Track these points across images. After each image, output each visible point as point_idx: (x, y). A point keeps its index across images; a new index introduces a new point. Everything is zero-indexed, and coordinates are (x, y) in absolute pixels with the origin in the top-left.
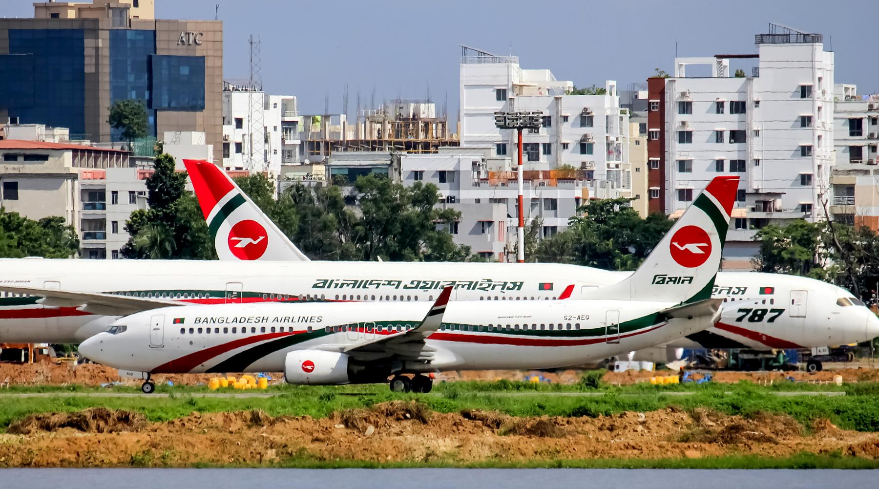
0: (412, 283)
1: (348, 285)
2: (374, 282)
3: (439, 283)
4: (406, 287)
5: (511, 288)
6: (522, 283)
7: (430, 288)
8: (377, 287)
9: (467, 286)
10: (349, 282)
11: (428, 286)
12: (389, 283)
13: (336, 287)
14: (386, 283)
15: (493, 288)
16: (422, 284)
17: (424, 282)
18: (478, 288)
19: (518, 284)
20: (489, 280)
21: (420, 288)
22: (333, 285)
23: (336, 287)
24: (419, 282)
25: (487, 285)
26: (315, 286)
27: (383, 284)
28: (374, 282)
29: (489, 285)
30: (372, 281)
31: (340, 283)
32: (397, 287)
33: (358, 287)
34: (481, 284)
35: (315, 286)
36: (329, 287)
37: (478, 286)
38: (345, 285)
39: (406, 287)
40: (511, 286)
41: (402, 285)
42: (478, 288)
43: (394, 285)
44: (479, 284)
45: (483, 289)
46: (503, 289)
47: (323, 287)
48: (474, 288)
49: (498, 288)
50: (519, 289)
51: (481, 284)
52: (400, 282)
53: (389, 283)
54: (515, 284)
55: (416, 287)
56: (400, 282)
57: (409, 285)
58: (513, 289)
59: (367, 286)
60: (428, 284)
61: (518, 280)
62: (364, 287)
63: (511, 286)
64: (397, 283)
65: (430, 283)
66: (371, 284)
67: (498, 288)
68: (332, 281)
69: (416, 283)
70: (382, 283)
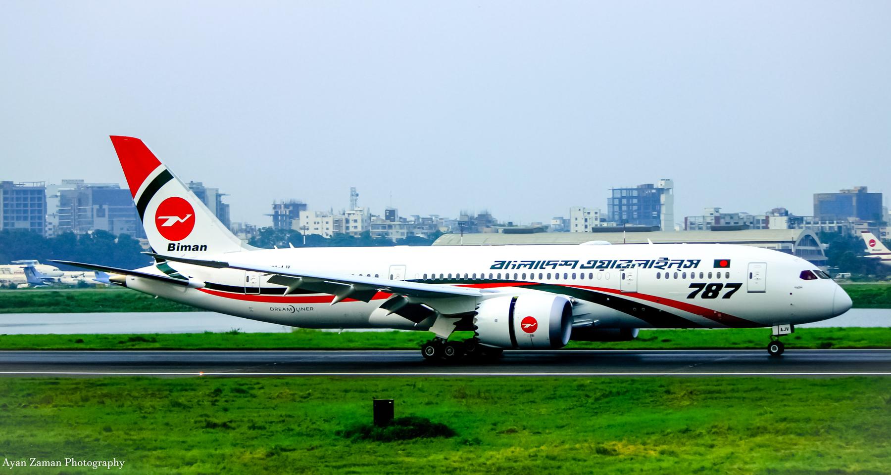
0: (589, 263)
1: (525, 266)
2: (551, 263)
3: (616, 261)
4: (582, 267)
5: (687, 265)
6: (699, 261)
7: (607, 267)
8: (554, 268)
9: (643, 265)
10: (526, 263)
11: (605, 265)
12: (566, 263)
13: (513, 268)
14: (563, 263)
15: (670, 267)
16: (598, 264)
17: (601, 262)
18: (655, 267)
19: (695, 262)
20: (666, 259)
21: (597, 268)
22: (511, 266)
23: (513, 268)
24: (596, 262)
25: (663, 264)
26: (493, 267)
27: (561, 265)
28: (551, 263)
29: (666, 263)
30: (549, 262)
31: (517, 264)
32: (574, 267)
33: (536, 268)
34: (658, 263)
35: (493, 267)
36: (506, 268)
37: (654, 264)
38: (523, 266)
39: (582, 267)
40: (688, 264)
41: (579, 265)
42: (655, 267)
43: (570, 265)
44: (655, 262)
45: (660, 267)
46: (679, 267)
47: (501, 268)
48: (650, 267)
49: (675, 266)
50: (696, 267)
51: (658, 263)
52: (576, 262)
53: (566, 263)
54: (691, 261)
55: (592, 267)
56: (576, 262)
57: (586, 265)
58: (689, 267)
59: (544, 266)
60: (604, 263)
61: (695, 258)
62: (541, 268)
63: (688, 264)
64: (573, 263)
65: (606, 263)
66: (548, 264)
67: (675, 266)
68: (510, 262)
70: (560, 263)
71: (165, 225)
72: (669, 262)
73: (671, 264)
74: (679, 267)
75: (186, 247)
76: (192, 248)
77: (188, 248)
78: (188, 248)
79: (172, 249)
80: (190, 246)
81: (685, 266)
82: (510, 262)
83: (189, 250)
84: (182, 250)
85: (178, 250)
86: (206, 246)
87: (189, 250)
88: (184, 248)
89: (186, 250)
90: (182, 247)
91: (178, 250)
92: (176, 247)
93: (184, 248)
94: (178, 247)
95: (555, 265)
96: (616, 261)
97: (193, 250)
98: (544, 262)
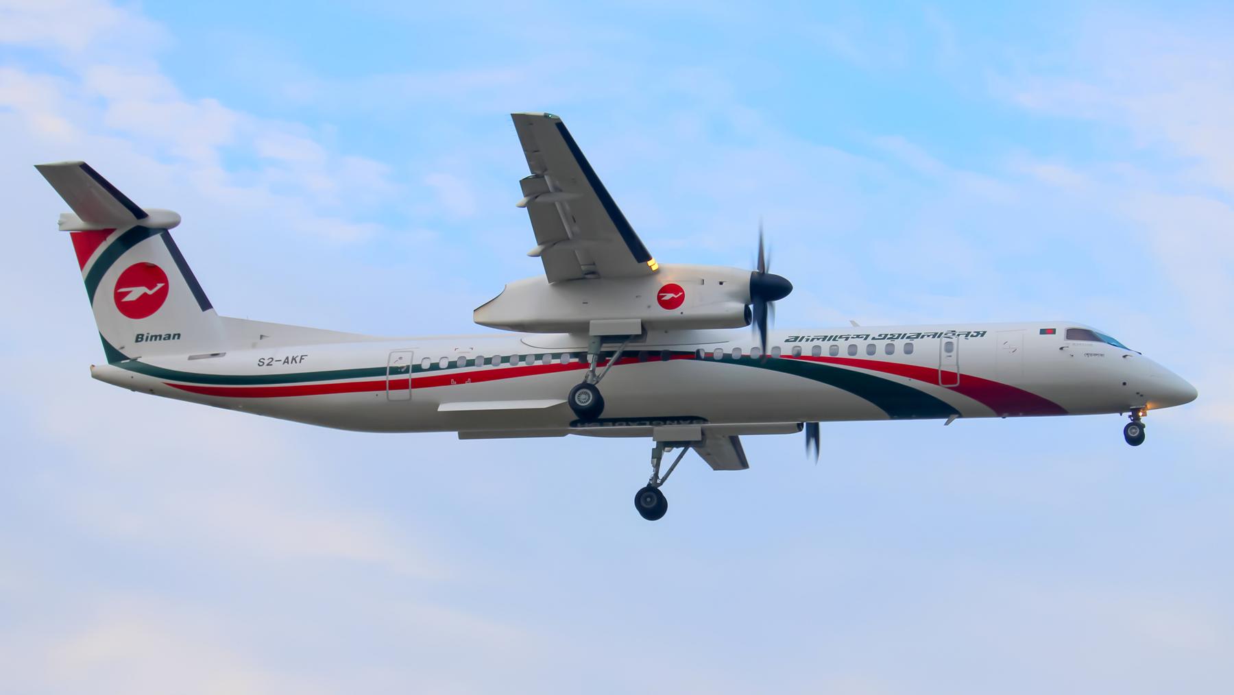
0: (880, 335)
1: (818, 339)
7: (898, 338)
12: (858, 336)
16: (889, 336)
22: (804, 340)
23: (807, 340)
24: (886, 335)
26: (787, 341)
32: (865, 339)
35: (787, 341)
37: (943, 335)
39: (874, 339)
46: (967, 336)
52: (868, 336)
53: (858, 336)
55: (884, 338)
56: (868, 336)
57: (877, 337)
58: (977, 336)
63: (975, 334)
65: (897, 336)
66: (841, 337)
67: (963, 337)
68: (803, 337)
69: (883, 336)
71: (127, 299)
72: (957, 334)
73: (959, 335)
74: (967, 336)
75: (156, 336)
76: (163, 337)
77: (158, 338)
78: (158, 338)
79: (140, 340)
80: (161, 336)
81: (972, 336)
82: (803, 337)
83: (160, 339)
84: (151, 340)
85: (147, 340)
86: (179, 335)
87: (160, 339)
88: (154, 338)
89: (156, 339)
90: (152, 337)
91: (147, 340)
92: (145, 338)
93: (154, 338)
94: (147, 337)
95: (847, 339)
96: (905, 334)
97: (164, 339)
98: (837, 336)
